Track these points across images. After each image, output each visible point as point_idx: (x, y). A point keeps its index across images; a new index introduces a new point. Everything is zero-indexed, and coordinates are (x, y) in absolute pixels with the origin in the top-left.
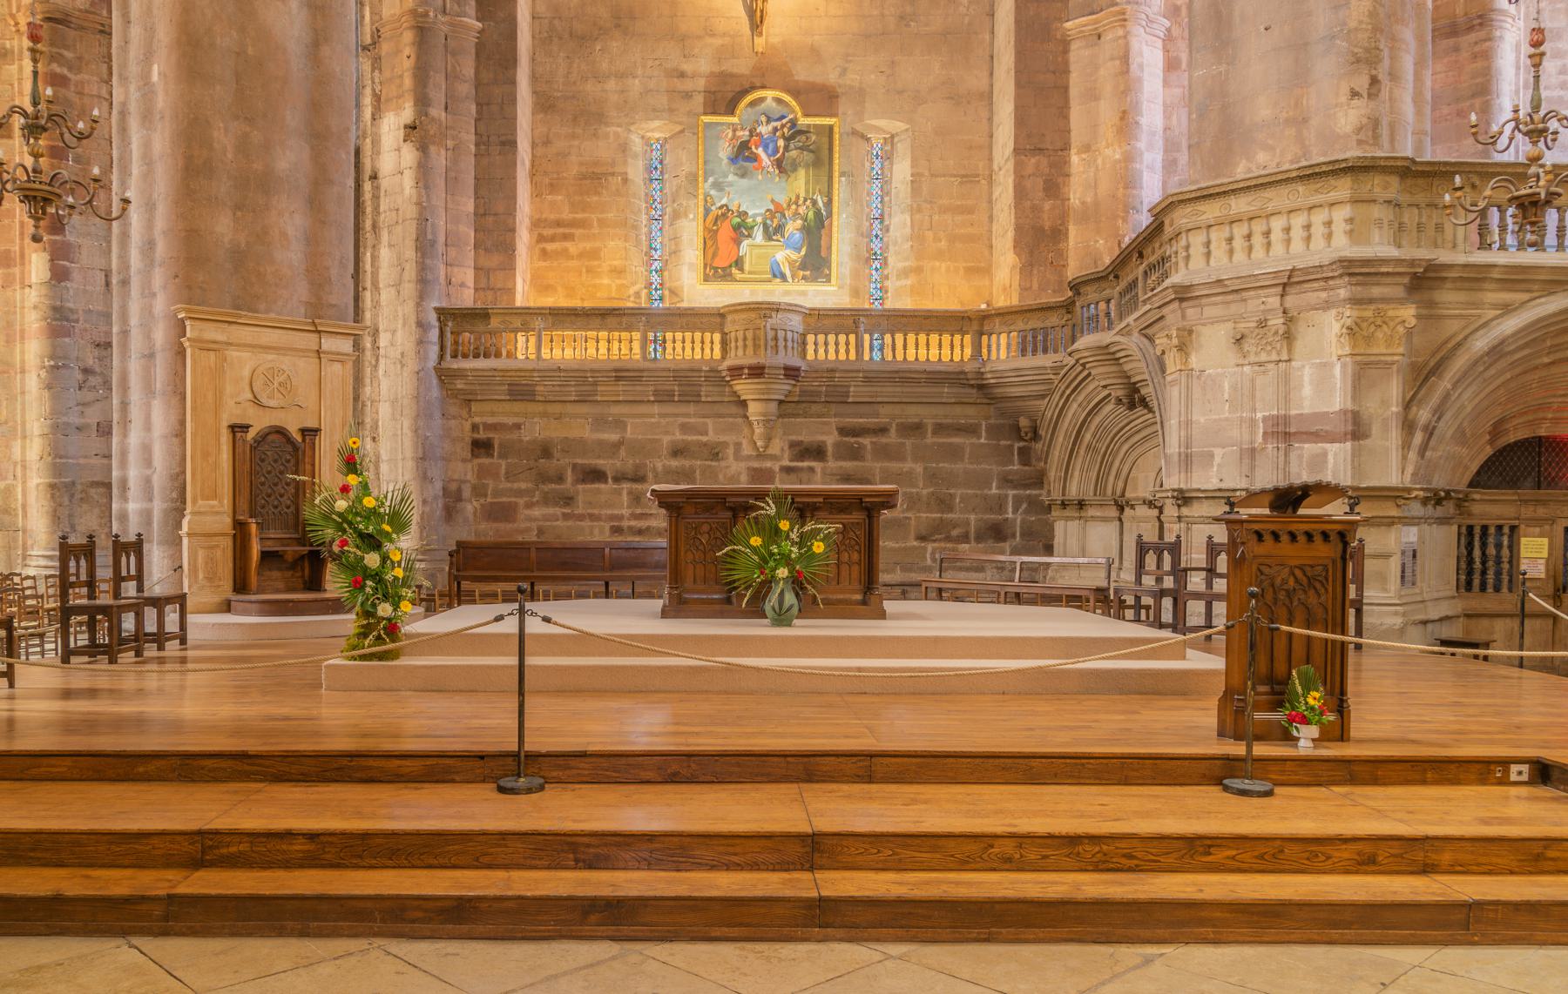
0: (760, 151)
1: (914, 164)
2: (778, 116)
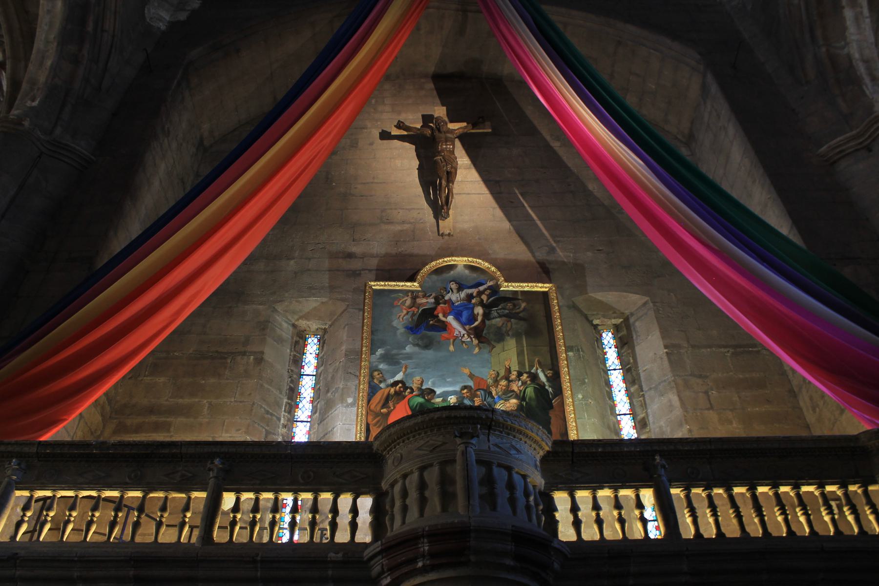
0: (450, 319)
1: (665, 334)
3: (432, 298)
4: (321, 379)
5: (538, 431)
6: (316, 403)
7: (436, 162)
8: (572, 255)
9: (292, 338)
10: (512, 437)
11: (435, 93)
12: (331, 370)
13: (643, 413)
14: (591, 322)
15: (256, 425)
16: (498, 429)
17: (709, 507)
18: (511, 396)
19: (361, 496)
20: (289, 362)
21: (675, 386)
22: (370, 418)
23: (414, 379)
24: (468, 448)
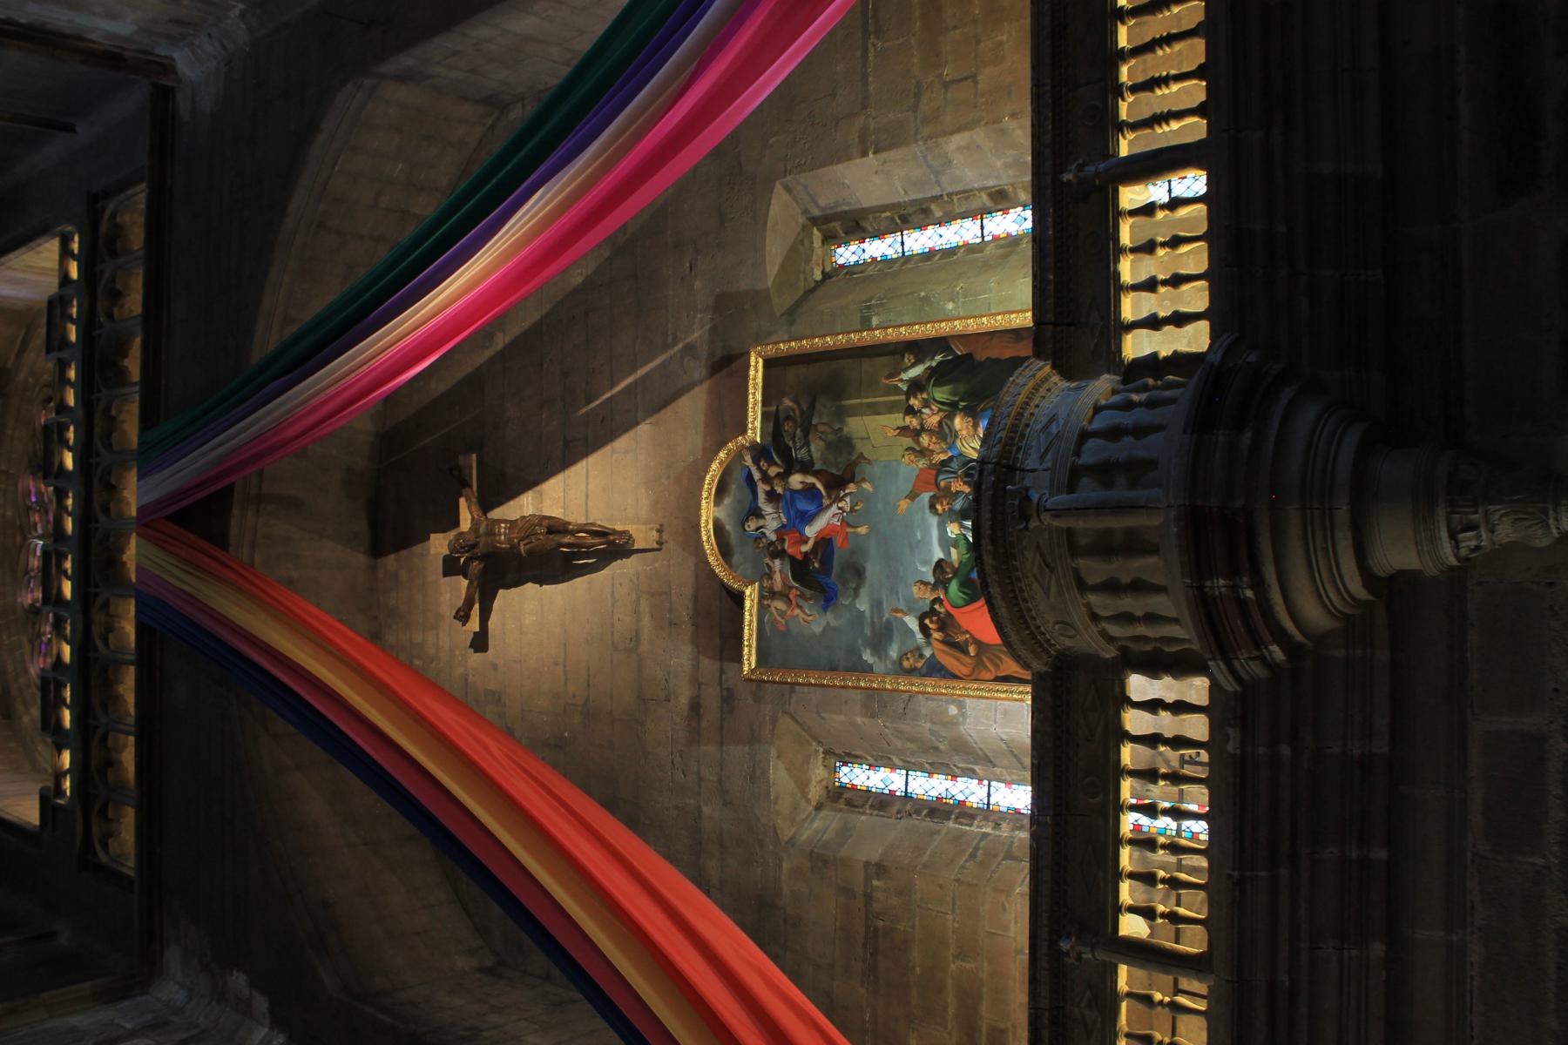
0: (811, 531)
1: (842, 156)
2: (747, 491)
3: (774, 563)
4: (913, 761)
5: (1017, 384)
6: (956, 770)
7: (530, 553)
8: (699, 316)
9: (840, 810)
10: (1029, 429)
11: (404, 553)
12: (899, 744)
13: (981, 197)
14: (818, 284)
15: (996, 876)
16: (1014, 453)
17: (1152, 90)
18: (947, 425)
19: (1128, 694)
20: (883, 816)
21: (934, 140)
22: (985, 675)
23: (916, 596)
24: (1048, 507)
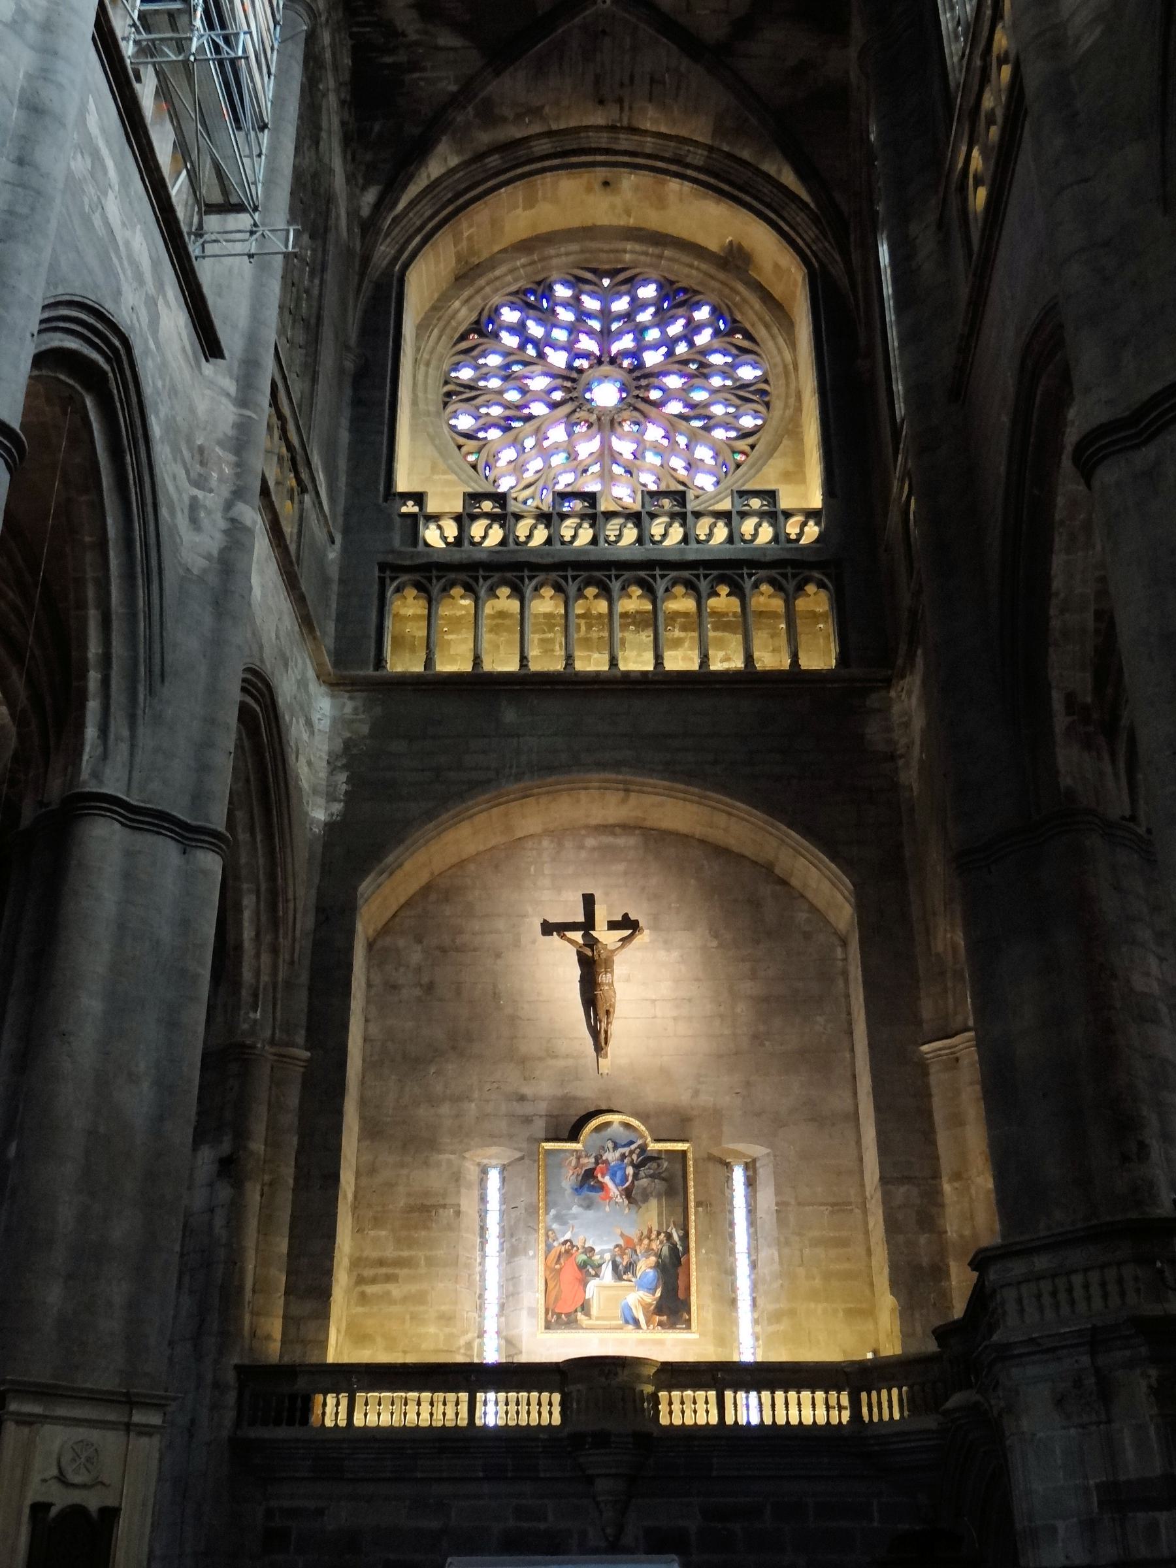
1: (778, 1192)
22: (548, 1273)
